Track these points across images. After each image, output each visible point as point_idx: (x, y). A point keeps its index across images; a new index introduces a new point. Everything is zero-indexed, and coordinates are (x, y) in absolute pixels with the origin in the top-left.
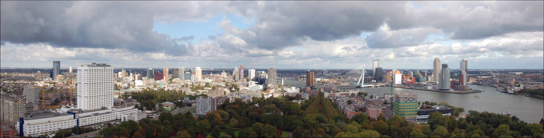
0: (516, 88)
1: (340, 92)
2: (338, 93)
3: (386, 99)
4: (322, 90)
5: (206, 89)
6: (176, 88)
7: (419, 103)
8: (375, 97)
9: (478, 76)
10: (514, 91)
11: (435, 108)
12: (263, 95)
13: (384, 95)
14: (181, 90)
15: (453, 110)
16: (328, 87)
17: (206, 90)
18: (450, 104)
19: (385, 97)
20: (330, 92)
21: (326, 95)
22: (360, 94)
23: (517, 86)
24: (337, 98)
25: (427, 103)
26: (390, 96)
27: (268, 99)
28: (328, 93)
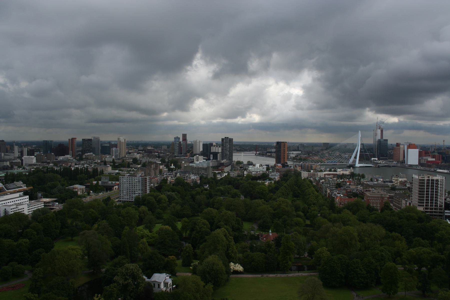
1: (325, 171)
3: (394, 183)
4: (299, 169)
5: (134, 167)
6: (88, 166)
8: (377, 180)
12: (215, 175)
13: (392, 177)
14: (97, 169)
16: (307, 165)
17: (133, 168)
19: (393, 181)
20: (311, 172)
21: (305, 175)
22: (352, 175)
24: (321, 178)
26: (400, 180)
27: (221, 179)
28: (307, 173)
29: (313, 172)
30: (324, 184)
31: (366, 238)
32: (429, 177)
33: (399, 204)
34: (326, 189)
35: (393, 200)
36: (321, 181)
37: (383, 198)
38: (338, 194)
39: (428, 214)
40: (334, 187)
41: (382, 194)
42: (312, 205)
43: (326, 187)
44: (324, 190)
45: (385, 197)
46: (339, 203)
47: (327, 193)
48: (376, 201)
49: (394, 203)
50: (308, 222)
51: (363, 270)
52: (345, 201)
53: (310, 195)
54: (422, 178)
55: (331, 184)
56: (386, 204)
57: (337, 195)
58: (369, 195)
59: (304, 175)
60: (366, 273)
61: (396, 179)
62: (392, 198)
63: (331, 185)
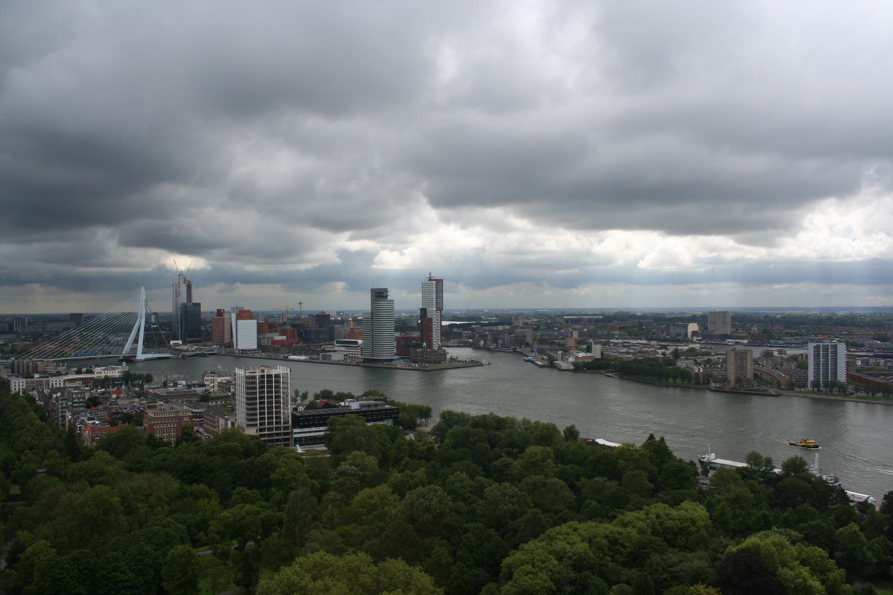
0: (581, 355)
1: (67, 374)
2: (58, 379)
3: (207, 388)
7: (304, 396)
8: (175, 385)
9: (473, 326)
10: (573, 364)
11: (348, 406)
13: (203, 376)
15: (398, 409)
18: (392, 397)
19: (206, 383)
20: (33, 378)
22: (127, 378)
23: (583, 351)
25: (326, 394)
26: (219, 379)
28: (24, 380)
29: (40, 377)
30: (60, 402)
31: (139, 505)
32: (263, 371)
33: (214, 427)
34: (65, 412)
35: (202, 421)
36: (54, 396)
37: (181, 418)
38: (89, 419)
39: (265, 441)
40: (81, 406)
41: (178, 412)
42: (27, 451)
43: (64, 408)
44: (60, 415)
45: (185, 416)
46: (90, 440)
47: (67, 421)
48: (167, 426)
49: (206, 426)
50: (15, 490)
51: (128, 571)
52: (102, 435)
53: (24, 428)
54: (250, 374)
55: (74, 401)
56: (186, 431)
57: (87, 422)
58: (153, 415)
59: (17, 385)
60: (134, 576)
61: (211, 378)
62: (202, 417)
63: (77, 403)
